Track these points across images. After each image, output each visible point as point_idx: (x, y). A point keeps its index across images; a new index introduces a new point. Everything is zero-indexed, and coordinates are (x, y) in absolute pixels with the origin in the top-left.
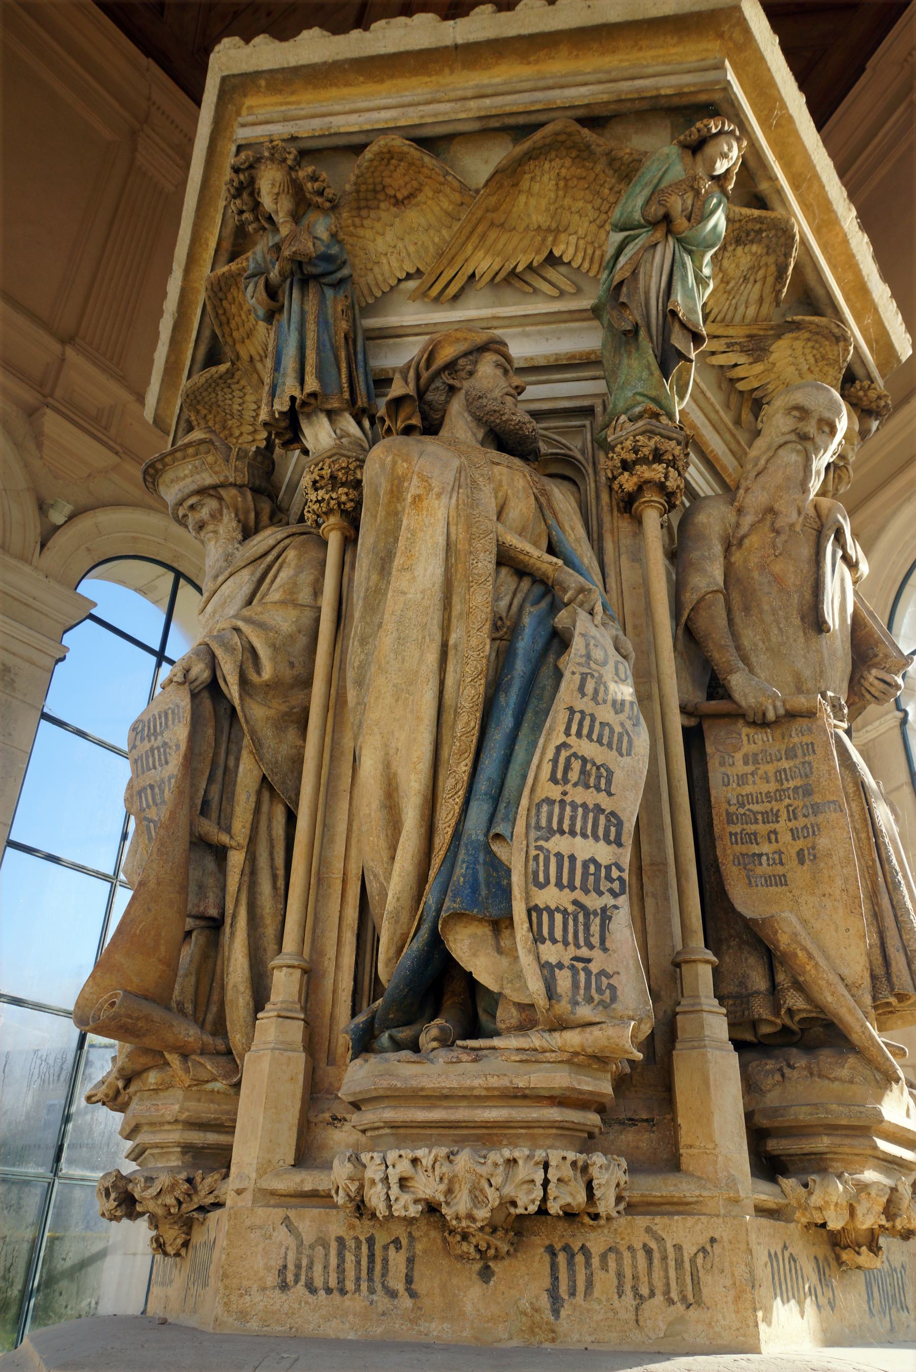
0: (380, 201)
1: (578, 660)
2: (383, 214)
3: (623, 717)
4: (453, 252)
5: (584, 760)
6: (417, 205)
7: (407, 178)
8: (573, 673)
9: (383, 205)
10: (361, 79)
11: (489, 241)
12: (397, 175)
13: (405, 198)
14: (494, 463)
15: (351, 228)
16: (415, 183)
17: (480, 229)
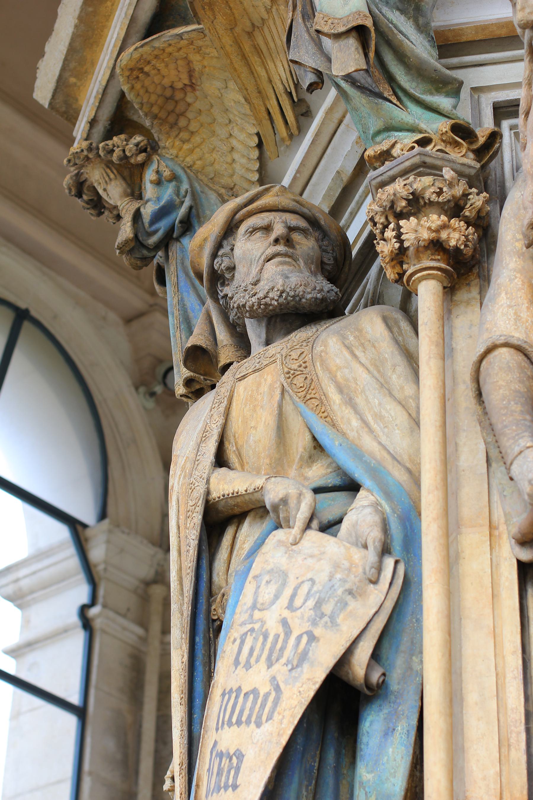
0: (183, 99)
1: (242, 620)
2: (198, 105)
3: (276, 667)
4: (251, 88)
5: (221, 755)
6: (202, 73)
7: (172, 66)
8: (235, 640)
9: (189, 99)
10: (109, 4)
11: (264, 50)
12: (164, 71)
13: (191, 80)
14: (240, 379)
15: (186, 147)
16: (180, 62)
17: (247, 47)
